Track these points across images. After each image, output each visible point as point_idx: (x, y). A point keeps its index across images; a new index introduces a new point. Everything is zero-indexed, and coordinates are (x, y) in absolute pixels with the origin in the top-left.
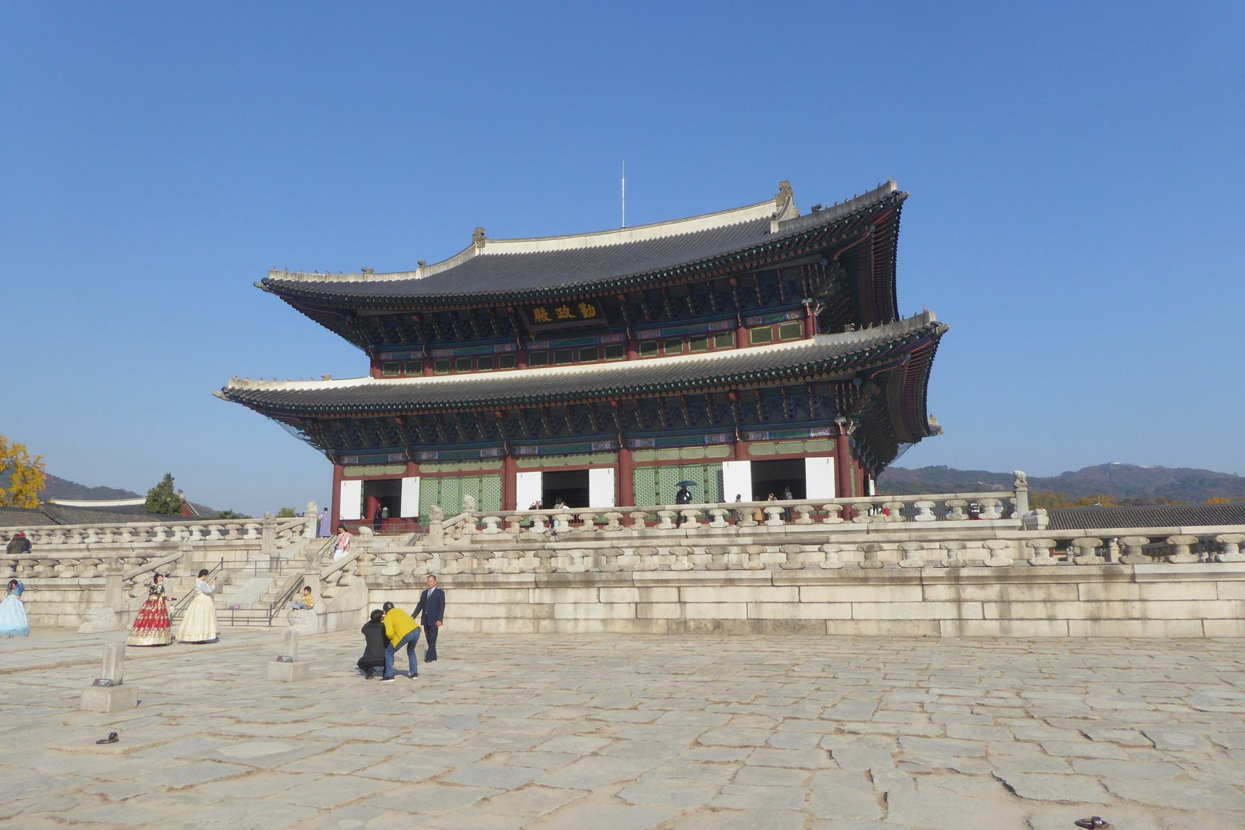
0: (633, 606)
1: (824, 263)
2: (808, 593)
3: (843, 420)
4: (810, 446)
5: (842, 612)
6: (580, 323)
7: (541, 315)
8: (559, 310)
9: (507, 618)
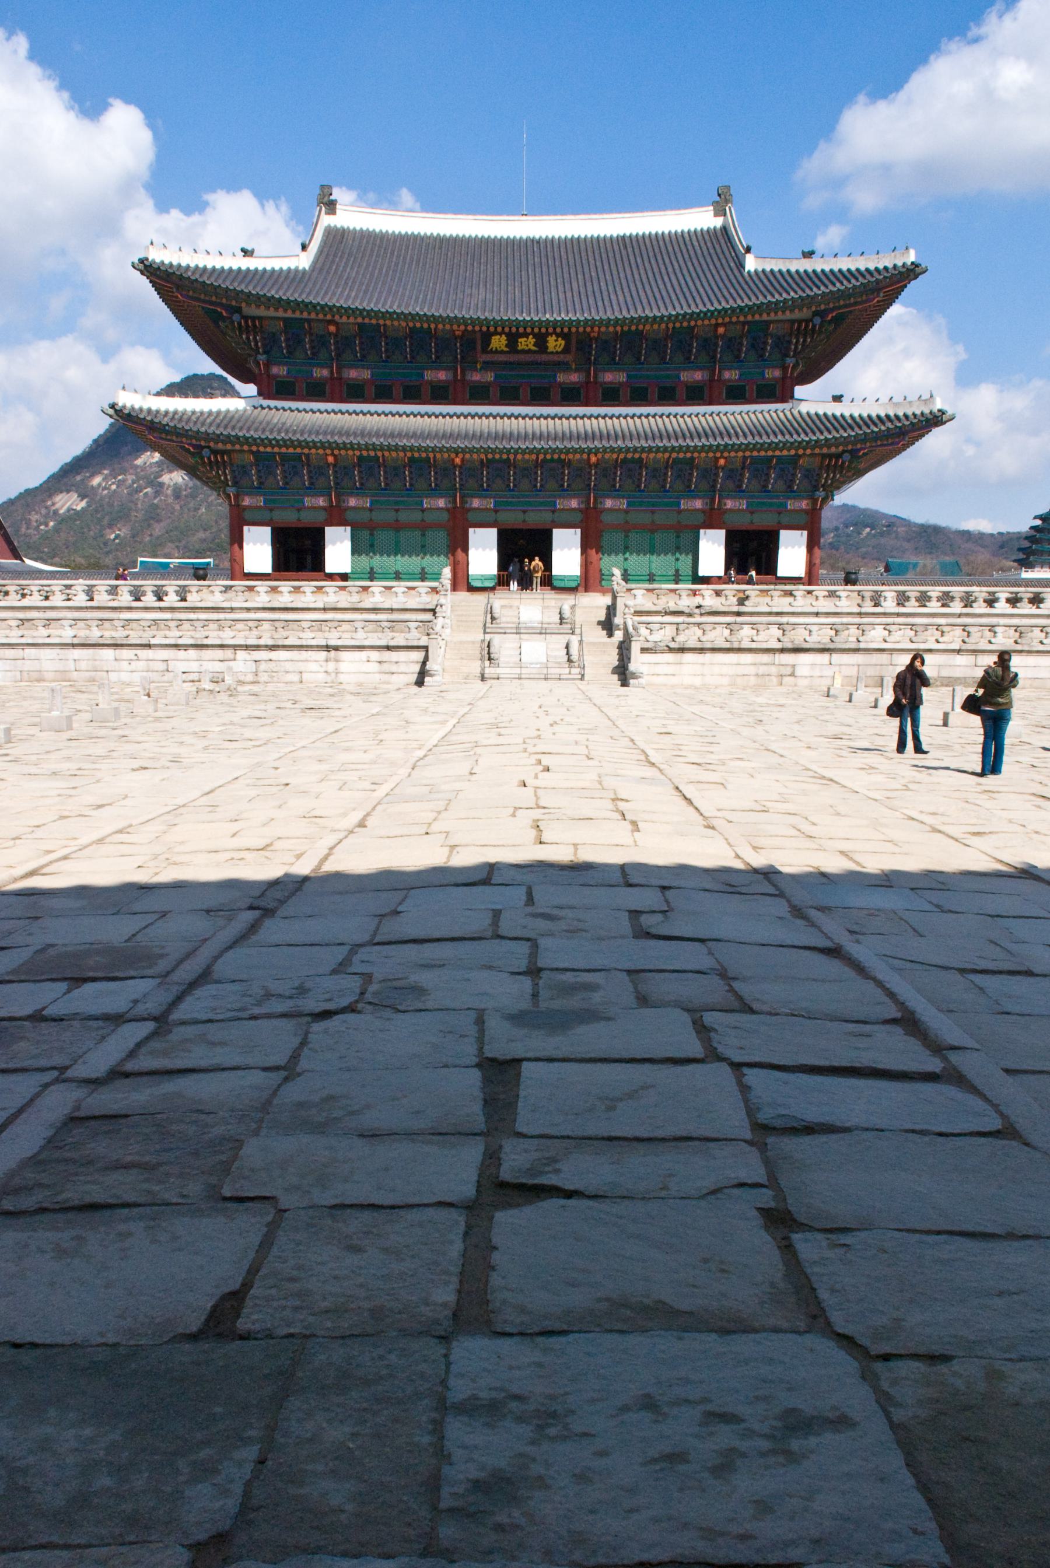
0: (856, 668)
1: (817, 320)
6: (544, 357)
7: (499, 342)
8: (522, 340)
9: (757, 675)
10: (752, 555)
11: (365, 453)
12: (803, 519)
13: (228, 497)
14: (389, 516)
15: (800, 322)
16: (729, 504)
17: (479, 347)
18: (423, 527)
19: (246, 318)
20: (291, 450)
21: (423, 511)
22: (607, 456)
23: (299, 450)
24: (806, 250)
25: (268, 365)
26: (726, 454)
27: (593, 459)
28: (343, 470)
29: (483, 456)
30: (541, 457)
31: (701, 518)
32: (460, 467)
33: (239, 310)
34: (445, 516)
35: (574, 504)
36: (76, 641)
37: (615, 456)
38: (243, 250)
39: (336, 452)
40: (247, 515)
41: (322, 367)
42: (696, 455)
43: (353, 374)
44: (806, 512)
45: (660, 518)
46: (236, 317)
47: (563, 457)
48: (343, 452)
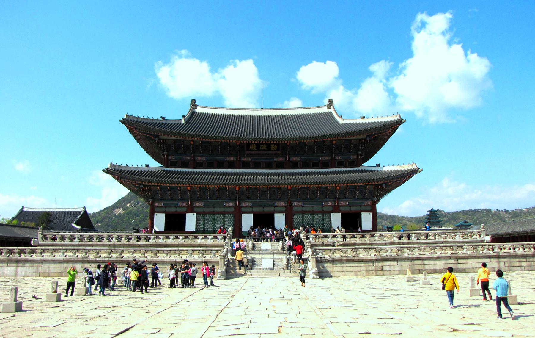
1: (368, 139)
2: (460, 261)
3: (376, 199)
4: (363, 208)
5: (469, 266)
7: (253, 147)
8: (262, 146)
9: (366, 271)
10: (351, 223)
11: (202, 186)
12: (369, 208)
13: (149, 203)
14: (212, 209)
15: (362, 139)
16: (342, 203)
17: (246, 149)
18: (224, 213)
19: (160, 139)
20: (173, 185)
21: (224, 207)
22: (295, 186)
23: (176, 185)
25: (167, 156)
26: (340, 185)
27: (289, 187)
28: (193, 192)
29: (247, 187)
30: (269, 187)
31: (331, 209)
32: (239, 191)
33: (158, 136)
34: (232, 209)
35: (282, 204)
36: (65, 259)
37: (298, 186)
38: (162, 117)
39: (191, 185)
40: (156, 209)
41: (187, 156)
42: (328, 185)
43: (199, 158)
44: (370, 205)
45: (315, 209)
46: (157, 139)
47: (278, 186)
48: (193, 186)
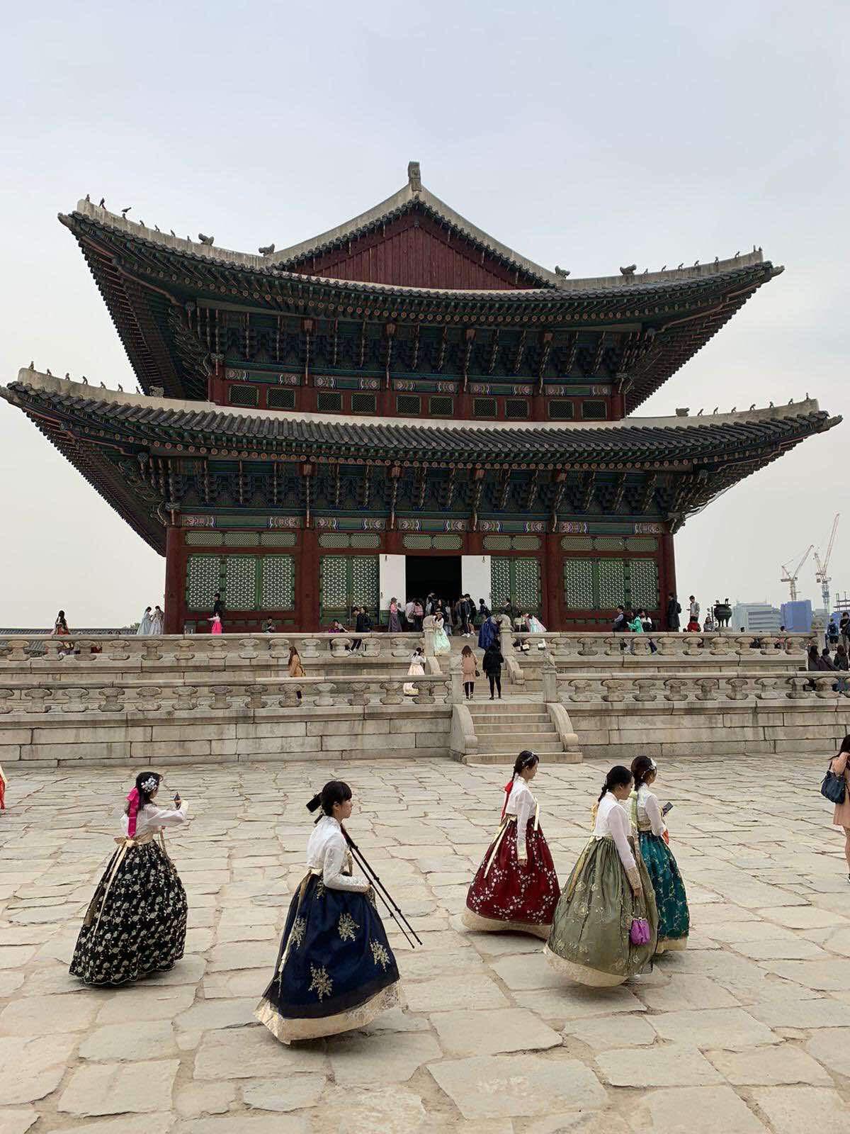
24: (625, 267)
